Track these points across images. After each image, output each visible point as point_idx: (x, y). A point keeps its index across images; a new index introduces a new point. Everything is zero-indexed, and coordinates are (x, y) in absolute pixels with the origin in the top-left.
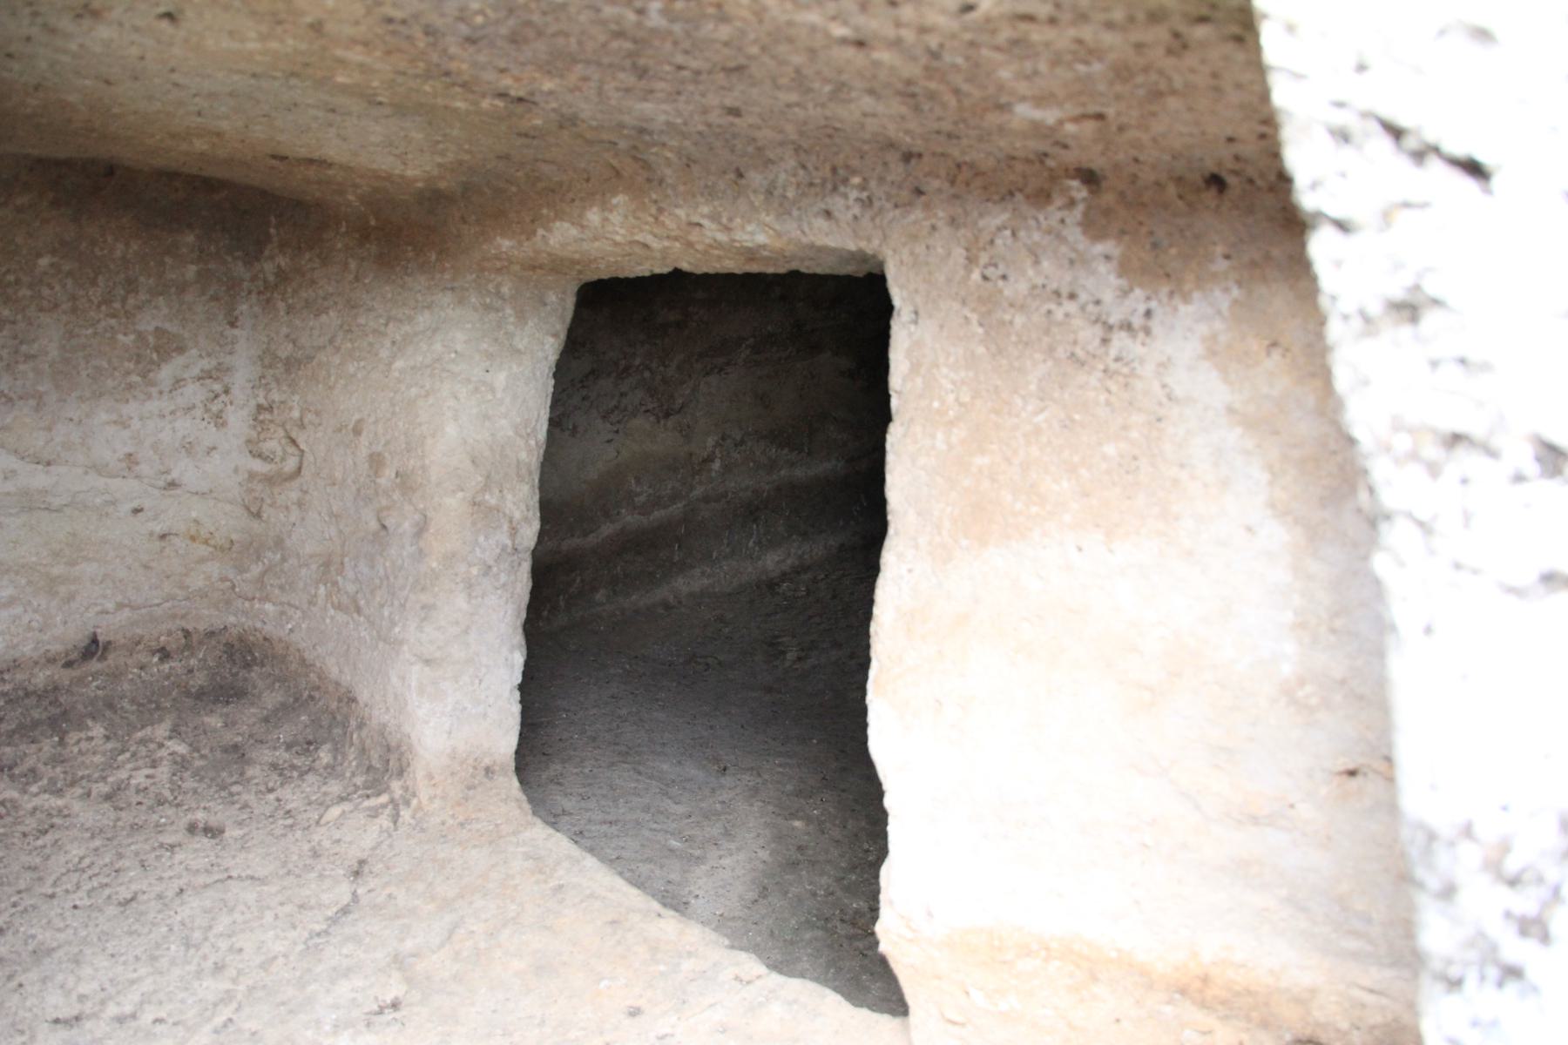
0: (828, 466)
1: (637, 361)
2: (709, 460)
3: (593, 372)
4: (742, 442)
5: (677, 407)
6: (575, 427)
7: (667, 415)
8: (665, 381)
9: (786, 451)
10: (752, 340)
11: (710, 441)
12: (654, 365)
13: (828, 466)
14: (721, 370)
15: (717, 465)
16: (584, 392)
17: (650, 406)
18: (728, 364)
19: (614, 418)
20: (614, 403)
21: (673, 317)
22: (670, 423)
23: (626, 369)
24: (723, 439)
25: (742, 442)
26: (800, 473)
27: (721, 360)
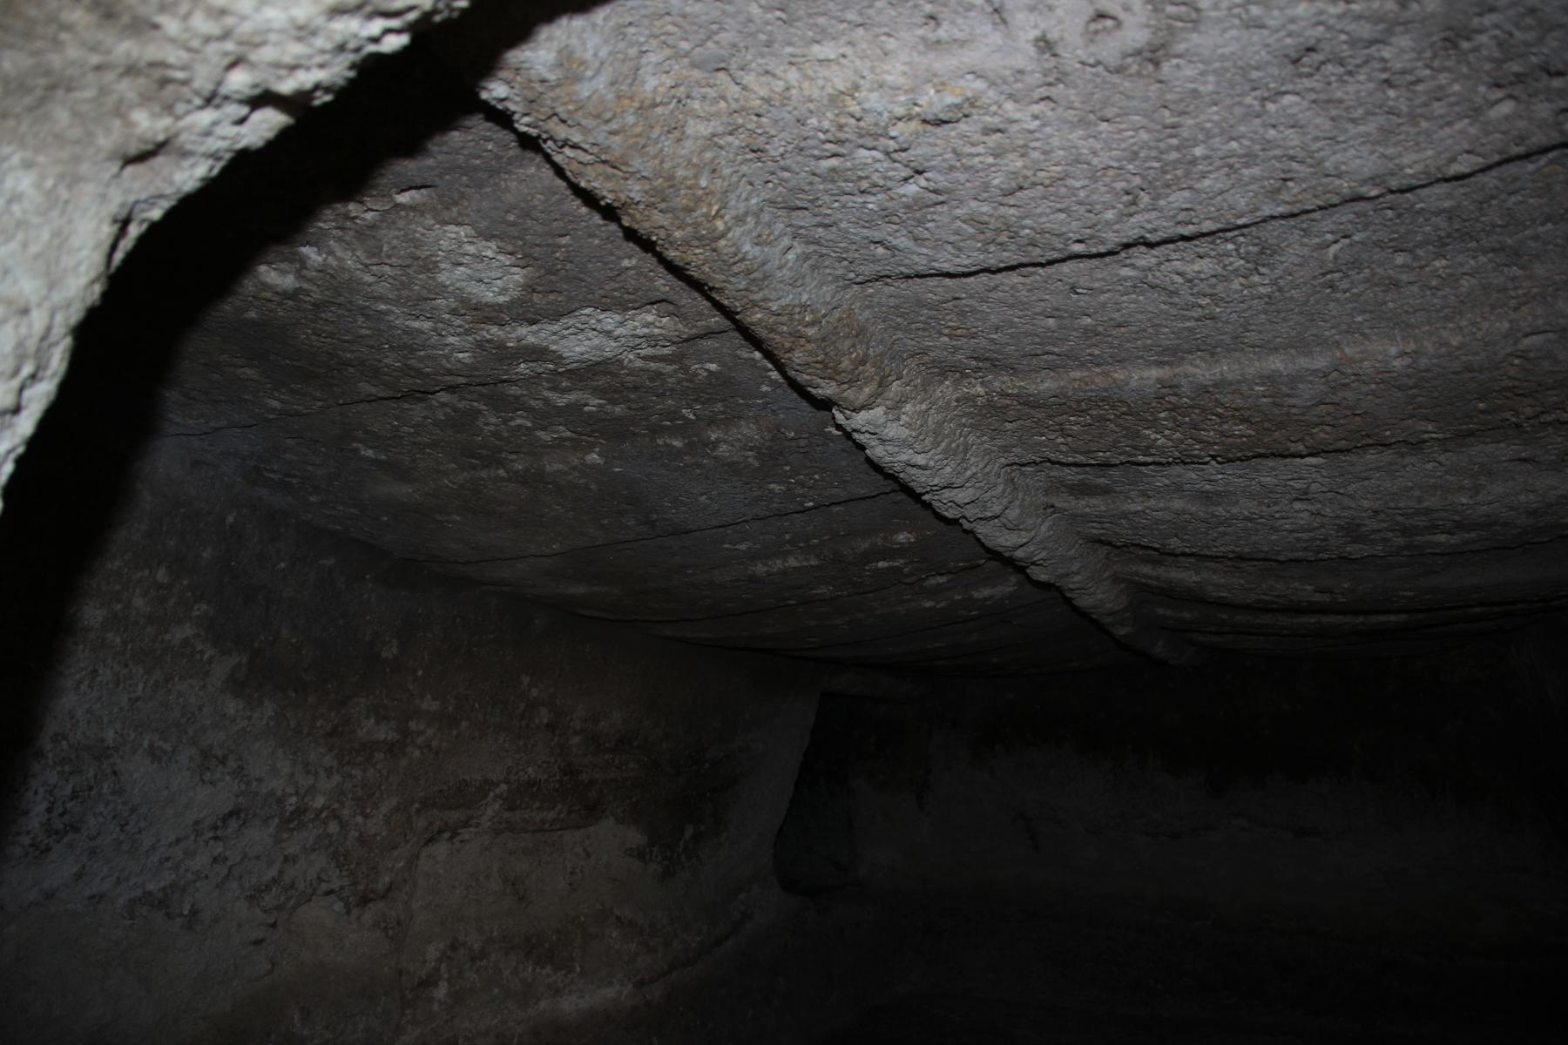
0: (610, 992)
1: (319, 802)
2: (429, 982)
3: (235, 813)
4: (483, 954)
5: (381, 887)
6: (194, 912)
7: (365, 901)
8: (362, 840)
9: (548, 969)
10: (504, 787)
11: (433, 952)
12: (346, 812)
13: (610, 992)
14: (454, 835)
15: (441, 992)
16: (219, 849)
17: (335, 885)
18: (466, 824)
19: (269, 900)
20: (273, 872)
21: (385, 733)
22: (369, 916)
23: (300, 812)
24: (453, 947)
25: (483, 954)
26: (570, 1005)
27: (455, 816)
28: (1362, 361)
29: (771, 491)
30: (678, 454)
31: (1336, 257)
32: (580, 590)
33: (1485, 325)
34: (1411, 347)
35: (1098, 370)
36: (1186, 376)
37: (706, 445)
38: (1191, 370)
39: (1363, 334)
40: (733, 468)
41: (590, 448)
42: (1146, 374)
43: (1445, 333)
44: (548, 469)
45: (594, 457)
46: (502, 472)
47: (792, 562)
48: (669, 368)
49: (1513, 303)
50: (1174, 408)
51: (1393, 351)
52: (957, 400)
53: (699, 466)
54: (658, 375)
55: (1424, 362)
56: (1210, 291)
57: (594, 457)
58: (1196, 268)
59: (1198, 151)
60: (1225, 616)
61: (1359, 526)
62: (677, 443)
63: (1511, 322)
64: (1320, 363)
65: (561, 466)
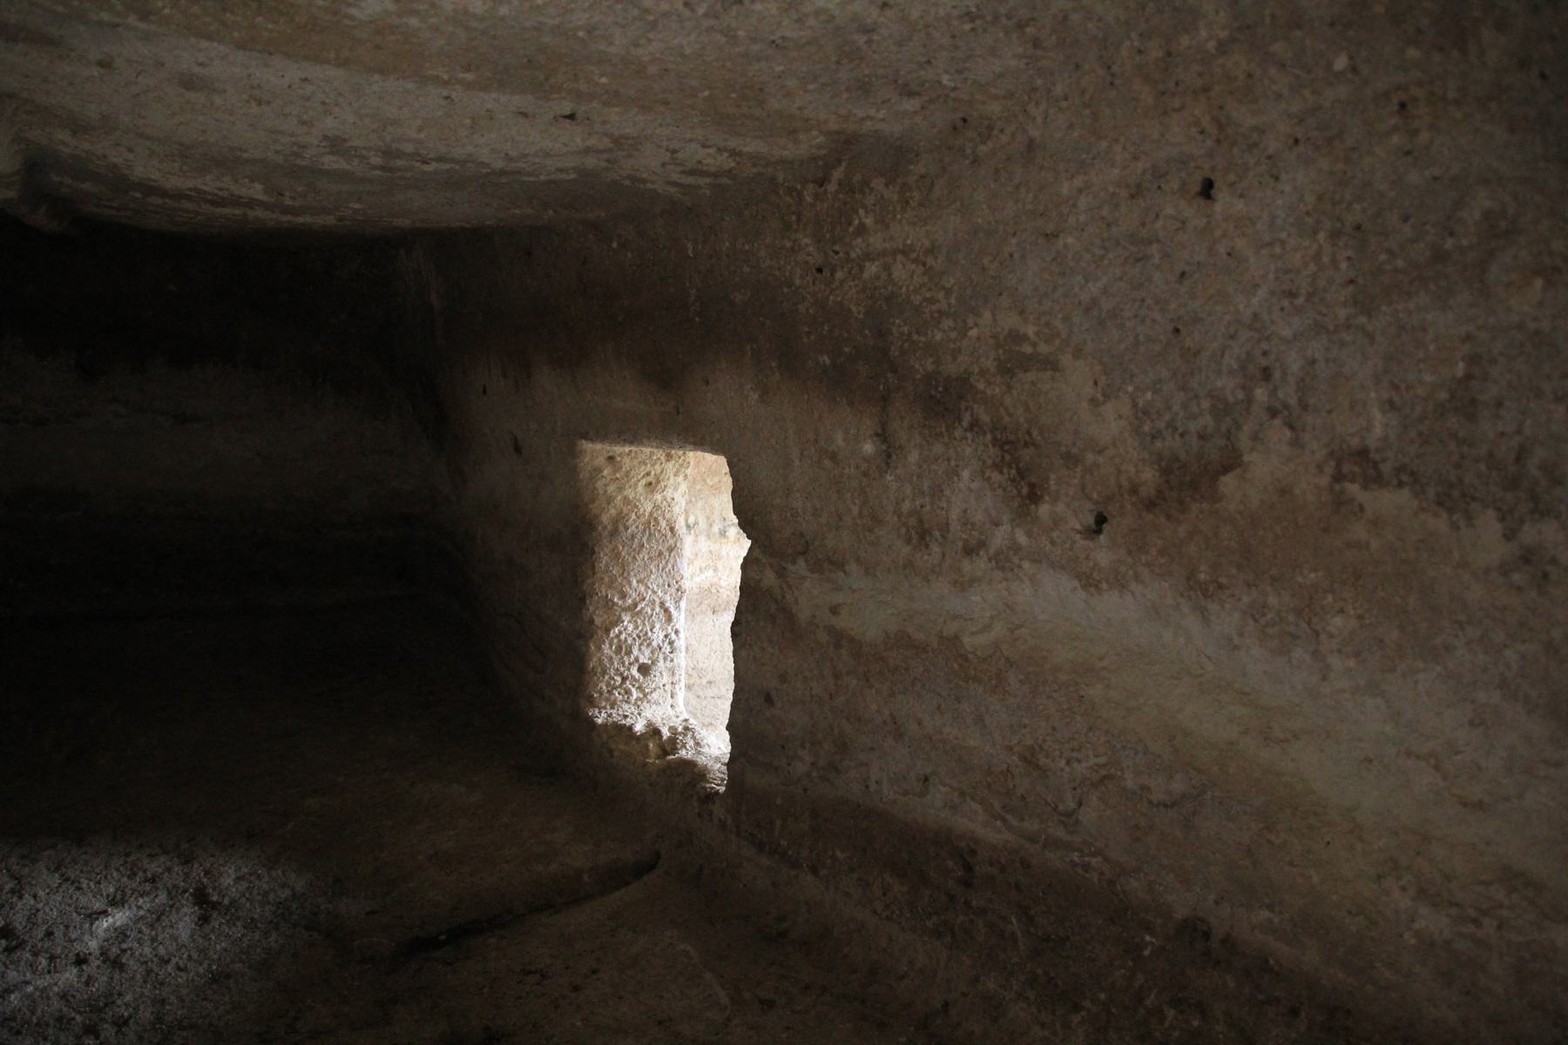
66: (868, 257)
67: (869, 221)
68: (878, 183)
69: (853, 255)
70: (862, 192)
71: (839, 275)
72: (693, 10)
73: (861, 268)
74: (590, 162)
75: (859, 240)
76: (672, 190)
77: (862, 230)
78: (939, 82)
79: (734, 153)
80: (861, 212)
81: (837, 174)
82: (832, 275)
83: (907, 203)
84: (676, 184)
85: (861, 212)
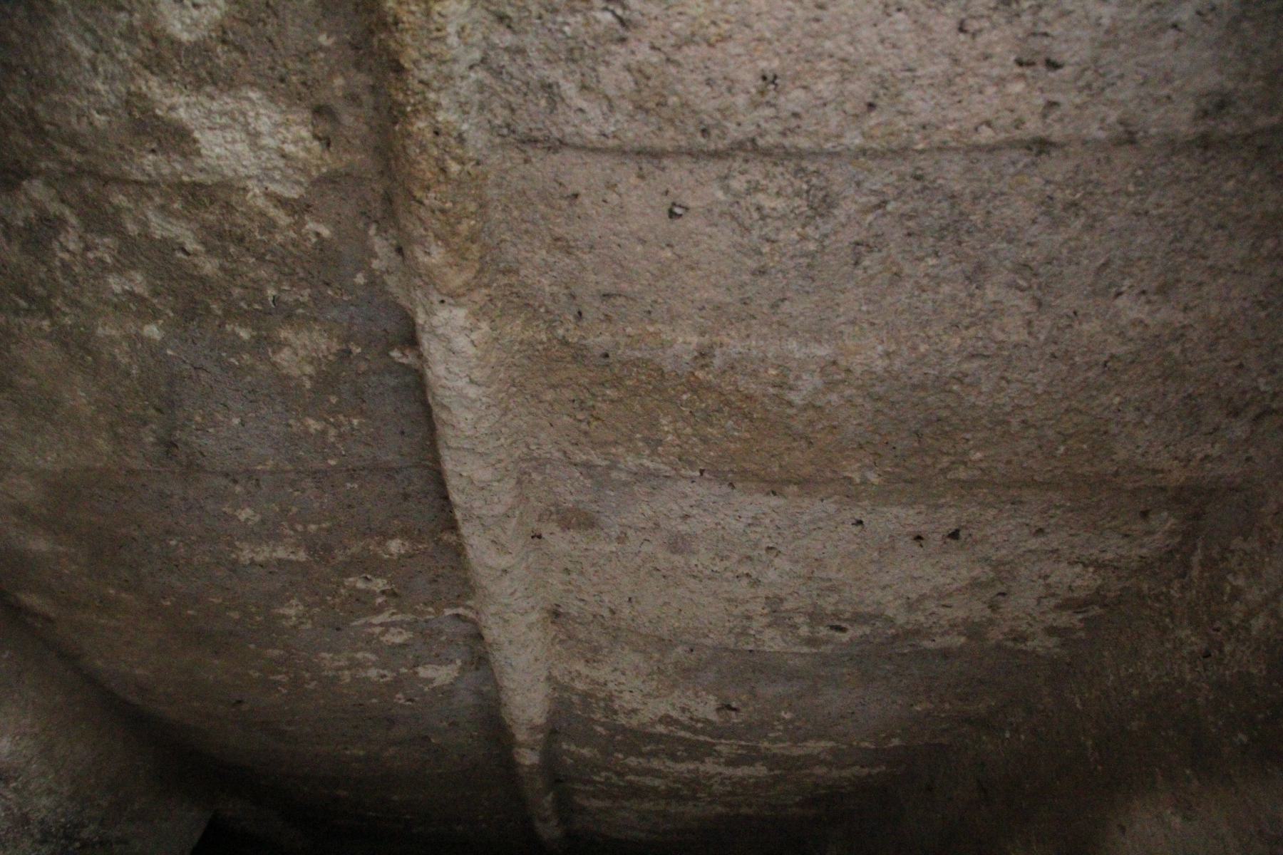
28: (856, 354)
29: (307, 427)
30: (237, 347)
31: (870, 224)
32: (40, 544)
33: (945, 338)
34: (893, 347)
35: (651, 329)
36: (721, 345)
37: (271, 345)
38: (726, 340)
39: (861, 329)
40: (284, 385)
41: (155, 315)
42: (689, 339)
43: (918, 341)
44: (100, 331)
45: (153, 331)
46: (46, 324)
47: (281, 553)
48: (283, 218)
49: (967, 321)
50: (696, 387)
51: (880, 348)
52: (521, 343)
53: (252, 368)
54: (270, 226)
55: (898, 364)
56: (773, 237)
57: (153, 331)
58: (773, 205)
59: (828, 45)
60: (620, 756)
61: (782, 600)
62: (244, 334)
63: (962, 339)
64: (823, 351)
65: (114, 332)
66: (1250, 614)
67: (1240, 582)
68: (1237, 542)
69: (1235, 622)
70: (1224, 559)
71: (1228, 648)
72: (1037, 338)
73: (1248, 630)
74: (978, 610)
75: (1237, 604)
76: (1052, 642)
77: (1236, 594)
78: (1257, 389)
79: (1099, 566)
80: (1230, 577)
81: (1196, 559)
82: (1221, 651)
83: (1271, 543)
84: (1051, 631)
85: (1230, 577)
